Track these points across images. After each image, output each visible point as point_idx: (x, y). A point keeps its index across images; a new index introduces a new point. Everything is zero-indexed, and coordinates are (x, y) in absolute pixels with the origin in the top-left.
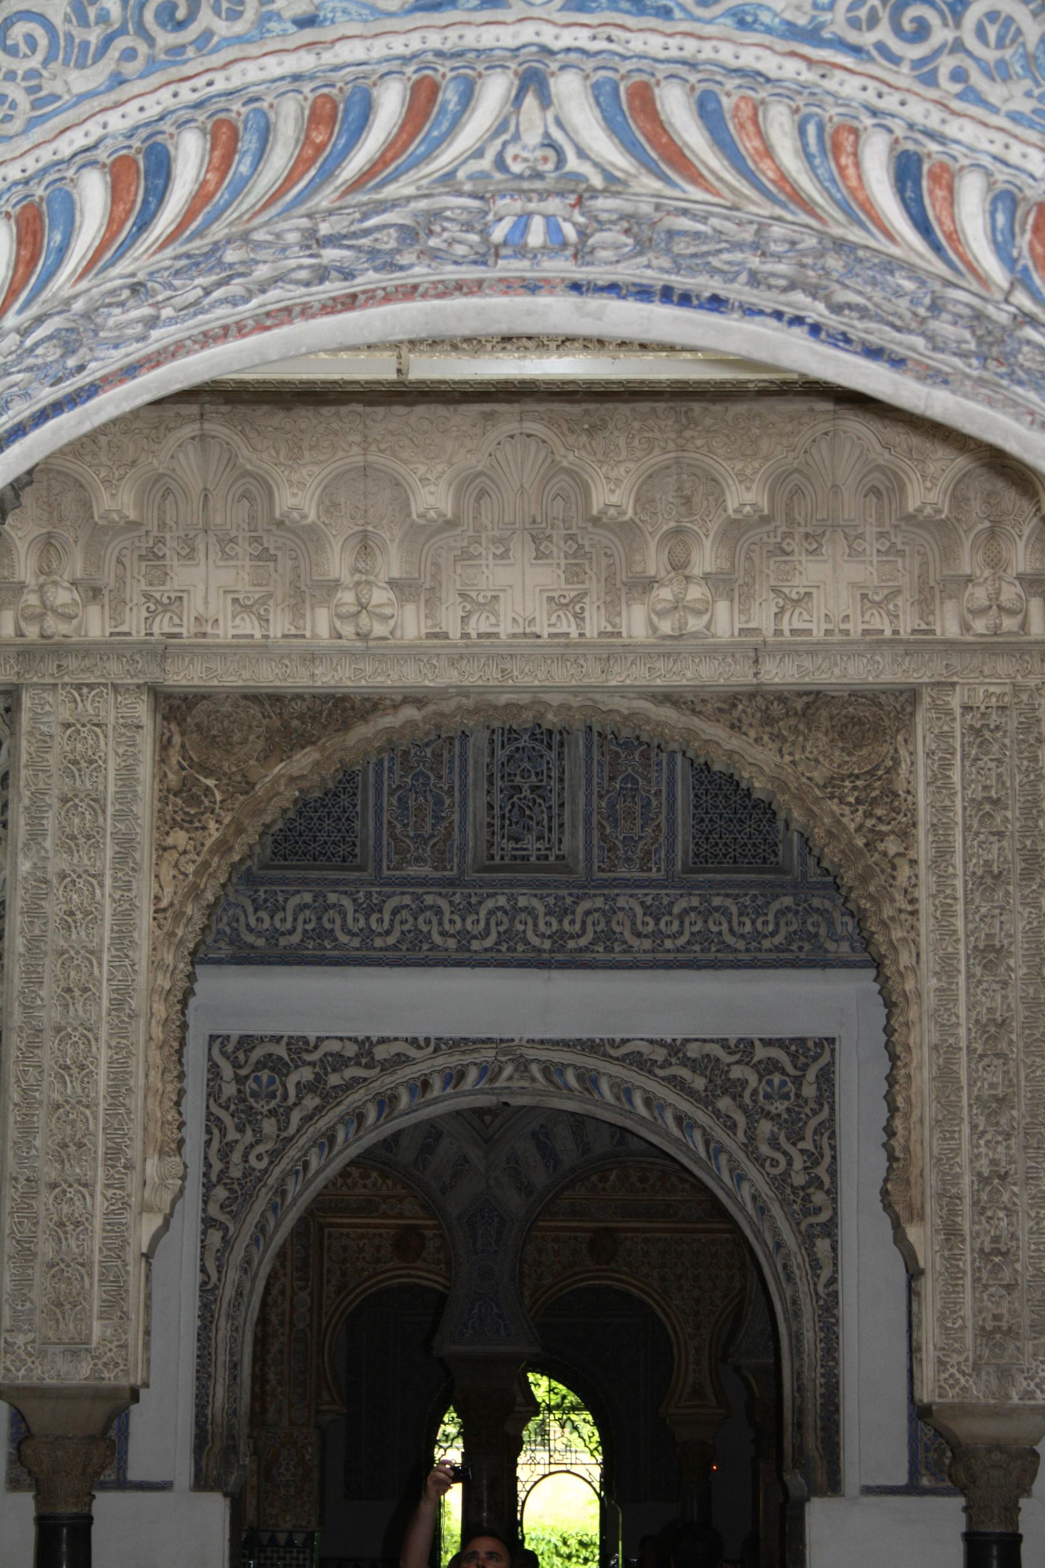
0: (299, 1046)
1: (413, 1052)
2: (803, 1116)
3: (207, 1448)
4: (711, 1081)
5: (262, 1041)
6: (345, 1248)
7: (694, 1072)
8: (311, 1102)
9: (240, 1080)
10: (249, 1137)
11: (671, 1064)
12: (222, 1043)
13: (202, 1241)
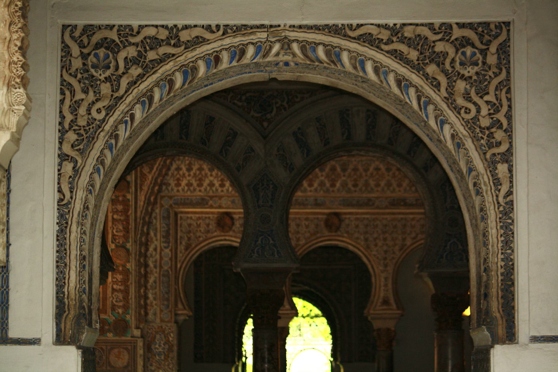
0: (126, 32)
1: (208, 35)
2: (487, 77)
3: (65, 315)
4: (421, 53)
5: (100, 28)
6: (190, 225)
7: (409, 47)
8: (136, 71)
9: (84, 56)
10: (91, 96)
11: (393, 42)
12: (72, 30)
13: (59, 170)
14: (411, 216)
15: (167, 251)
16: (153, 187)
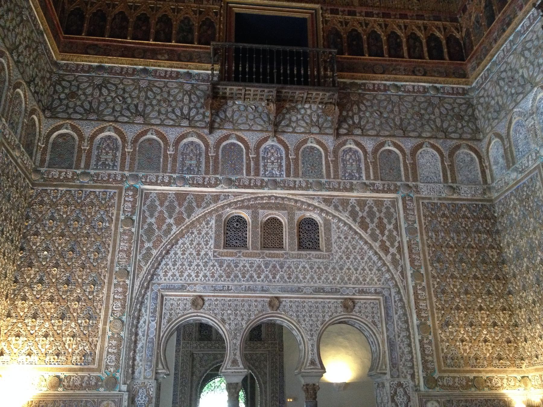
6: (172, 305)
14: (328, 300)
15: (154, 323)
16: (147, 276)
